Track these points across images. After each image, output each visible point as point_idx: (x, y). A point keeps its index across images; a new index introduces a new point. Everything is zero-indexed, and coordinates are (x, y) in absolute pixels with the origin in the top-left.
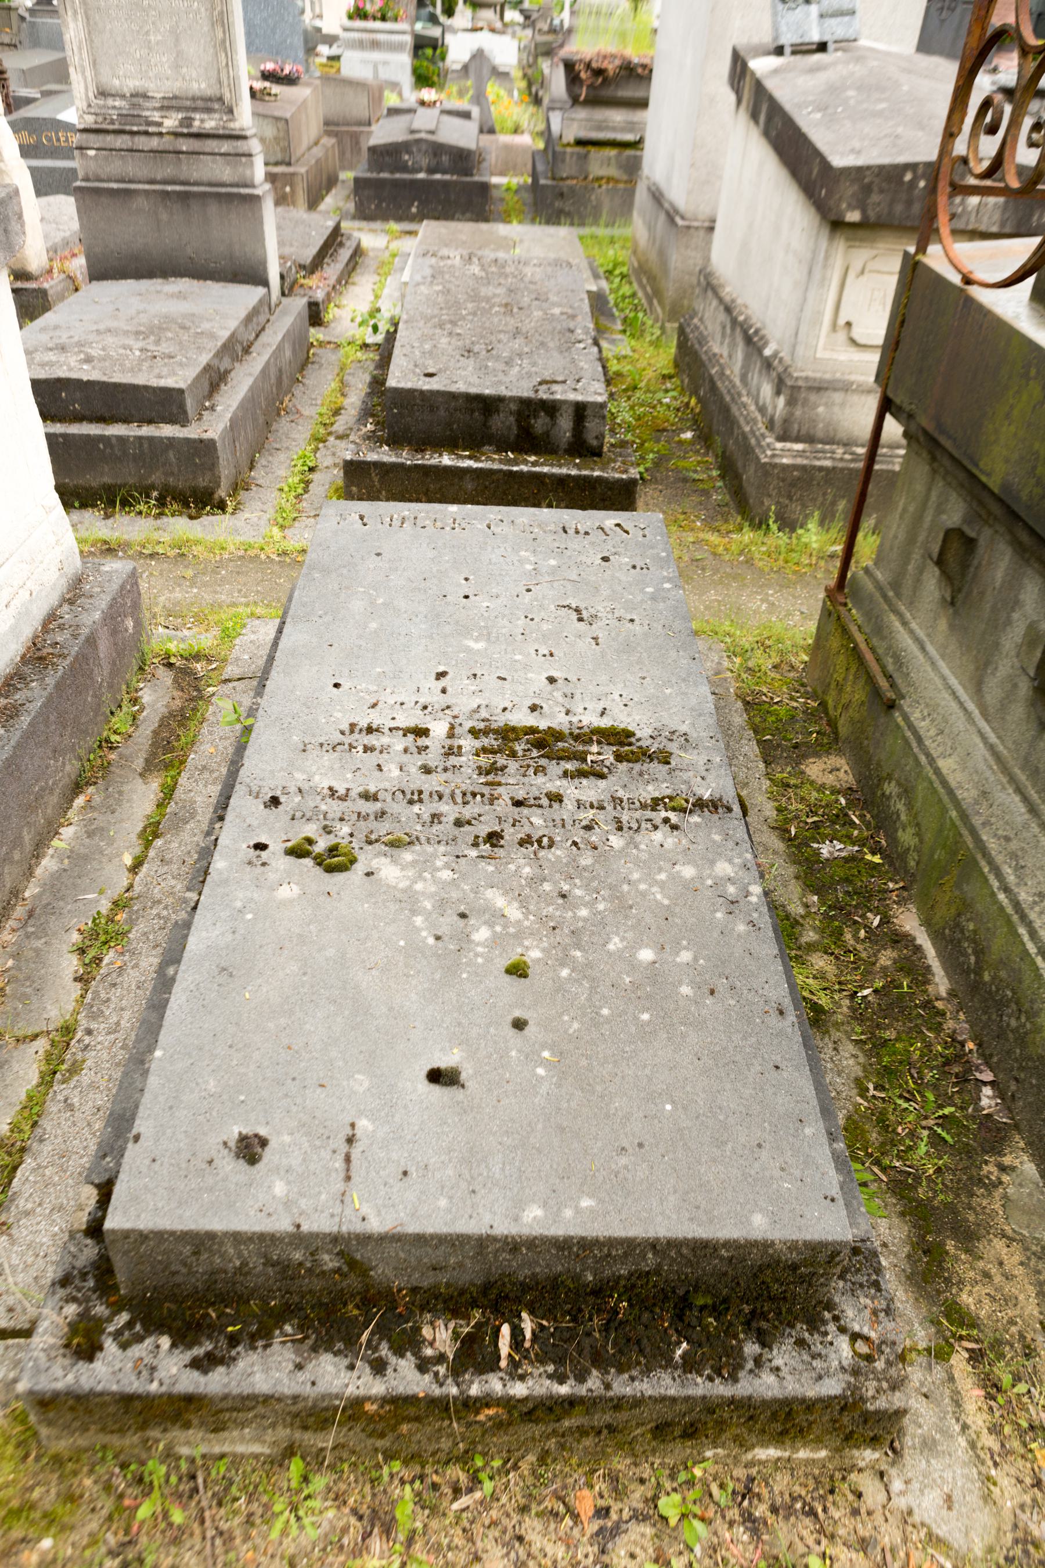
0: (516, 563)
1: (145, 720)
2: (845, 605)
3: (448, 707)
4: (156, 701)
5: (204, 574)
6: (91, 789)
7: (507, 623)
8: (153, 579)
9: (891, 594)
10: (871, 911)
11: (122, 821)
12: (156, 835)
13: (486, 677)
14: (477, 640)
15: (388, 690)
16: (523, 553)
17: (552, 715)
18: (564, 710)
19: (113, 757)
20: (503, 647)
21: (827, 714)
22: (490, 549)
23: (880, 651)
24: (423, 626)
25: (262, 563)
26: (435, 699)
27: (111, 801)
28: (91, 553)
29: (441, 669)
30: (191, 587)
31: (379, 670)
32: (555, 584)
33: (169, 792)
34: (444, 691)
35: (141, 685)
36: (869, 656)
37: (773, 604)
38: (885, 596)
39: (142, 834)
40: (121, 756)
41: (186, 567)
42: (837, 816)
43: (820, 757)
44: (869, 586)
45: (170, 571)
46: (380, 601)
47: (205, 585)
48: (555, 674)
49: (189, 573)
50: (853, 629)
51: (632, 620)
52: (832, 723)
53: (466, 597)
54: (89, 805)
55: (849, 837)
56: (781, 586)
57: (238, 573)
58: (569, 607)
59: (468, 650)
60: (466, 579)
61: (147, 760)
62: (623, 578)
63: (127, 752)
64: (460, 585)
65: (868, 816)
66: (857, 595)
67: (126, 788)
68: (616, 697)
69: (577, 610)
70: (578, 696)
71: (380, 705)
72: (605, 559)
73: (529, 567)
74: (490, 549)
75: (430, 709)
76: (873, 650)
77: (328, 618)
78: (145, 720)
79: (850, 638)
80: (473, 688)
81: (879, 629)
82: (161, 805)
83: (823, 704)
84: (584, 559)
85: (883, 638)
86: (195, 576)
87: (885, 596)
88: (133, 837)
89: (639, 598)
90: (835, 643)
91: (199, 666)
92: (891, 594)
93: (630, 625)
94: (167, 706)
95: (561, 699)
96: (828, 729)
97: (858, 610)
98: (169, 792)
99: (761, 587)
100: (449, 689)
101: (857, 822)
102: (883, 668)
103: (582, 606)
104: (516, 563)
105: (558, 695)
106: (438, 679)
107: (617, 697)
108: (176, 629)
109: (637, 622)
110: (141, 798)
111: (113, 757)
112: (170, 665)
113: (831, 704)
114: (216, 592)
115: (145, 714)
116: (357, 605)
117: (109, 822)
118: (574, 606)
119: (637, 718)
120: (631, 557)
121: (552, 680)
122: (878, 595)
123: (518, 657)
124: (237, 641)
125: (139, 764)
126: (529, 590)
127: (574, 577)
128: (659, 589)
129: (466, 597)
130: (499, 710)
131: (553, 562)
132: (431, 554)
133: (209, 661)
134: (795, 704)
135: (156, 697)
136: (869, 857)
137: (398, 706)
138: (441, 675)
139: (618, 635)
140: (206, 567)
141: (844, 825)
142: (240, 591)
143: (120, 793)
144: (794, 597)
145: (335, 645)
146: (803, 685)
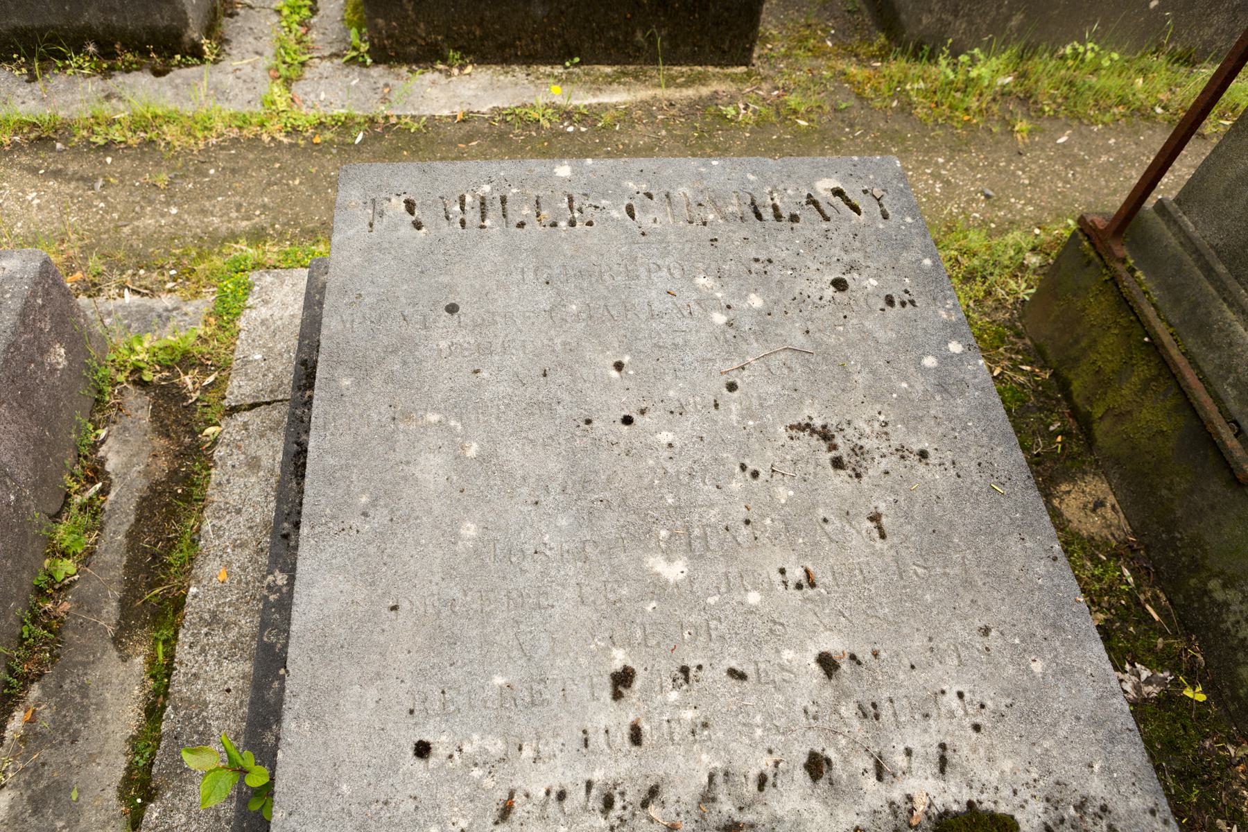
0: (695, 307)
1: (113, 511)
2: (1124, 261)
3: (654, 792)
4: (128, 465)
5: (184, 177)
6: (35, 691)
7: (716, 496)
8: (111, 191)
9: (1221, 268)
10: (1219, 814)
11: (91, 758)
12: (150, 796)
13: (706, 673)
14: (669, 555)
15: (528, 752)
16: (701, 281)
17: (857, 793)
18: (870, 764)
19: (66, 606)
20: (721, 569)
21: (1068, 397)
22: (642, 272)
23: (1208, 368)
24: (563, 522)
25: (266, 149)
26: (624, 766)
27: (70, 714)
28: (15, 145)
29: (619, 659)
30: (168, 204)
31: (499, 680)
32: (775, 362)
33: (162, 672)
34: (636, 736)
35: (103, 433)
36: (1190, 376)
37: (948, 182)
38: (1209, 271)
39: (123, 795)
40: (80, 602)
41: (157, 164)
42: (1127, 608)
43: (1072, 480)
44: (1171, 239)
45: (136, 175)
46: (473, 450)
47: (188, 197)
48: (834, 644)
49: (163, 179)
50: (1150, 312)
51: (923, 454)
52: (1085, 423)
53: (627, 420)
54: (31, 737)
55: (1151, 650)
56: (952, 149)
57: (233, 171)
58: (807, 427)
59: (659, 589)
60: (619, 366)
61: (123, 603)
62: (880, 334)
63: (88, 590)
64: (608, 385)
65: (1163, 597)
66: (1144, 245)
67: (93, 676)
68: (951, 700)
69: (826, 435)
70: (886, 712)
71: (519, 811)
72: (840, 285)
73: (720, 318)
74: (642, 272)
75: (618, 804)
76: (1193, 362)
77: (380, 517)
78: (113, 511)
79: (1140, 321)
80: (689, 715)
81: (1199, 325)
82: (153, 712)
83: (1065, 386)
84: (801, 285)
85: (1212, 347)
86: (171, 183)
87: (1209, 271)
88: (112, 794)
89: (919, 387)
90: (1097, 308)
91: (187, 380)
92: (1221, 268)
93: (921, 468)
94: (146, 473)
95: (857, 727)
96: (1072, 425)
97: (1146, 273)
98: (162, 672)
99: (927, 152)
100: (645, 727)
101: (1156, 617)
102: (1218, 400)
103: (833, 422)
104: (695, 307)
105: (848, 710)
106: (617, 696)
107: (955, 703)
108: (152, 293)
109: (933, 459)
110: (119, 686)
111: (66, 606)
112: (141, 384)
113: (1076, 386)
114: (203, 212)
115: (112, 496)
116: (431, 468)
117: (69, 767)
118: (818, 423)
119: (1007, 765)
120: (878, 277)
121: (827, 663)
122: (1189, 260)
123: (754, 598)
124: (242, 323)
125: (111, 610)
126: (732, 387)
127: (799, 340)
128: (946, 359)
129: (627, 420)
130: (752, 787)
131: (756, 301)
132: (545, 299)
133: (205, 370)
134: (1022, 379)
135: (128, 455)
136: (1188, 693)
137: (553, 807)
138: (623, 679)
139: (910, 500)
140: (185, 164)
141: (1139, 622)
142: (239, 207)
143: (84, 689)
144: (972, 168)
145: (405, 605)
146: (1019, 335)
